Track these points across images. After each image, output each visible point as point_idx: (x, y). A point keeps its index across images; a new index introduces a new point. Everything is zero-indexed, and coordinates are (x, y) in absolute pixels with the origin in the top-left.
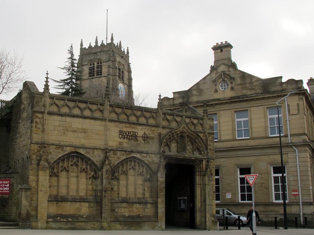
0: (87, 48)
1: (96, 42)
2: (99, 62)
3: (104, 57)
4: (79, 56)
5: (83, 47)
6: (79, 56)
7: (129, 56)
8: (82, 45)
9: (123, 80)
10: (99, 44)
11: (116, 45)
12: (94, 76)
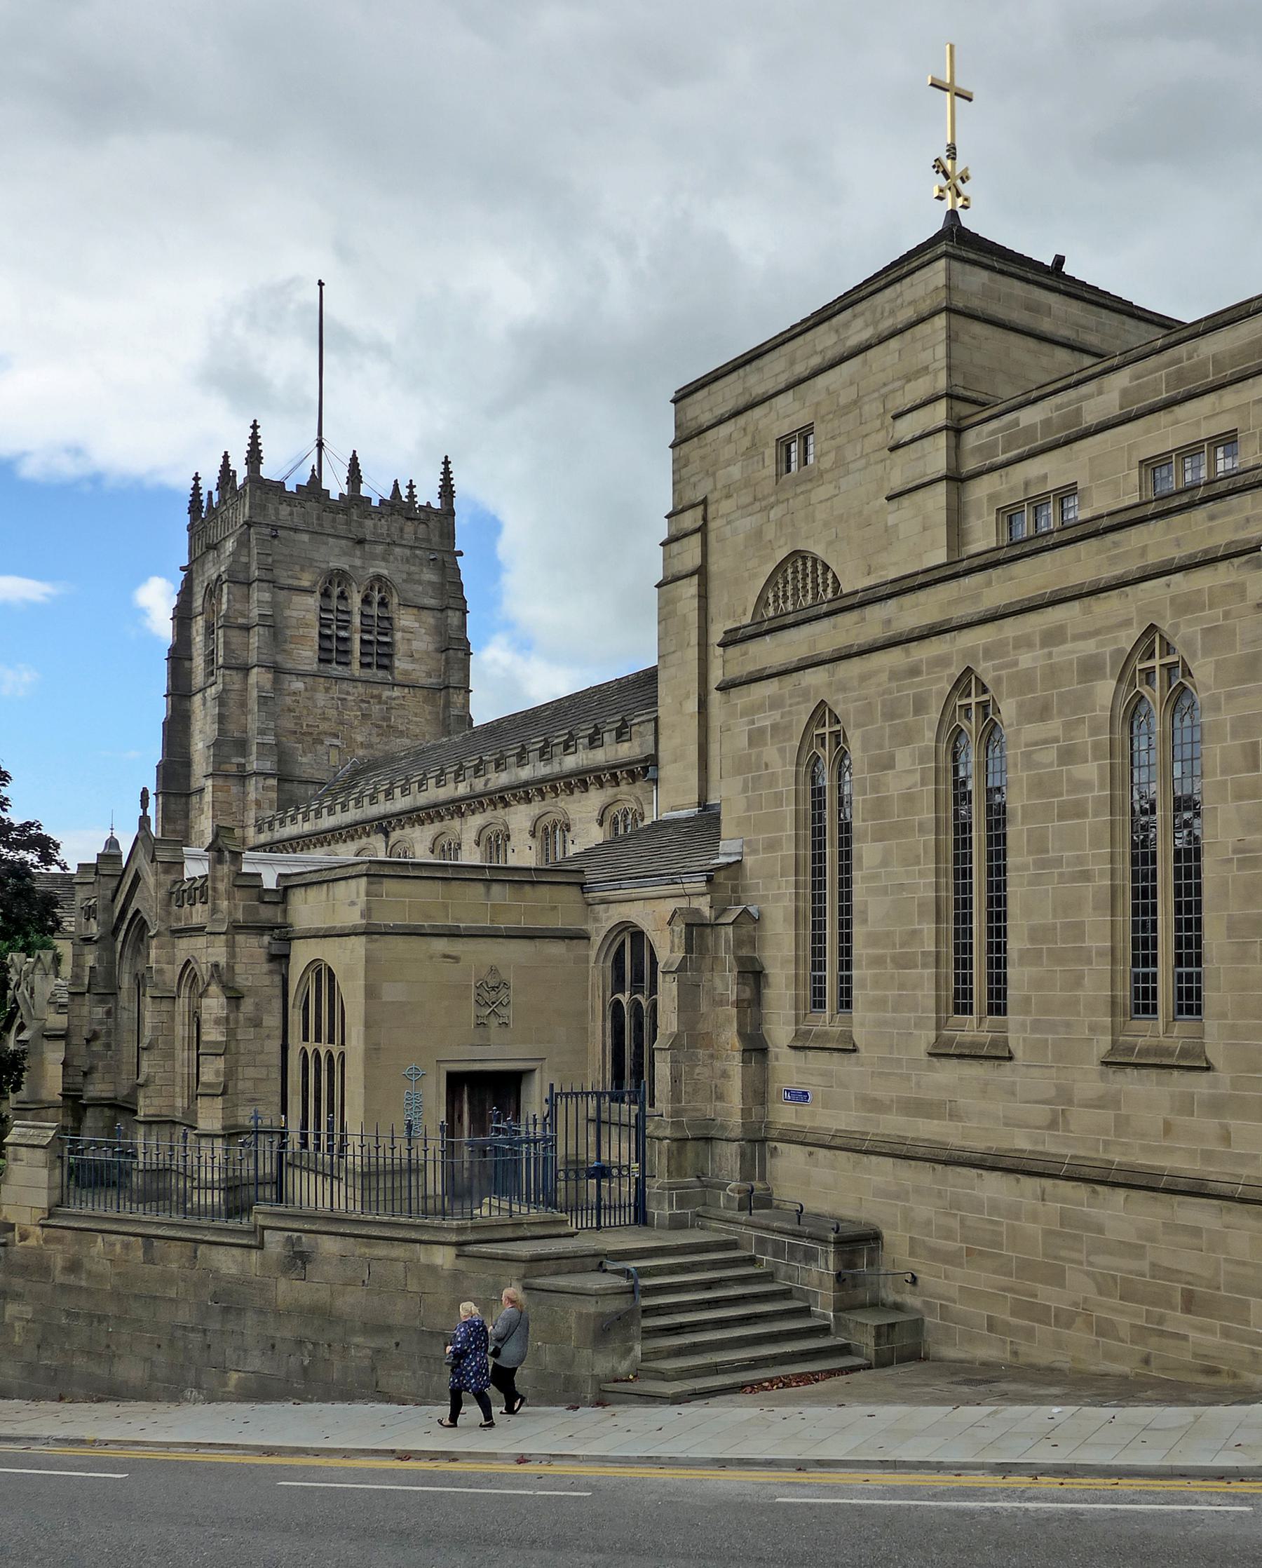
0: (290, 487)
2: (376, 597)
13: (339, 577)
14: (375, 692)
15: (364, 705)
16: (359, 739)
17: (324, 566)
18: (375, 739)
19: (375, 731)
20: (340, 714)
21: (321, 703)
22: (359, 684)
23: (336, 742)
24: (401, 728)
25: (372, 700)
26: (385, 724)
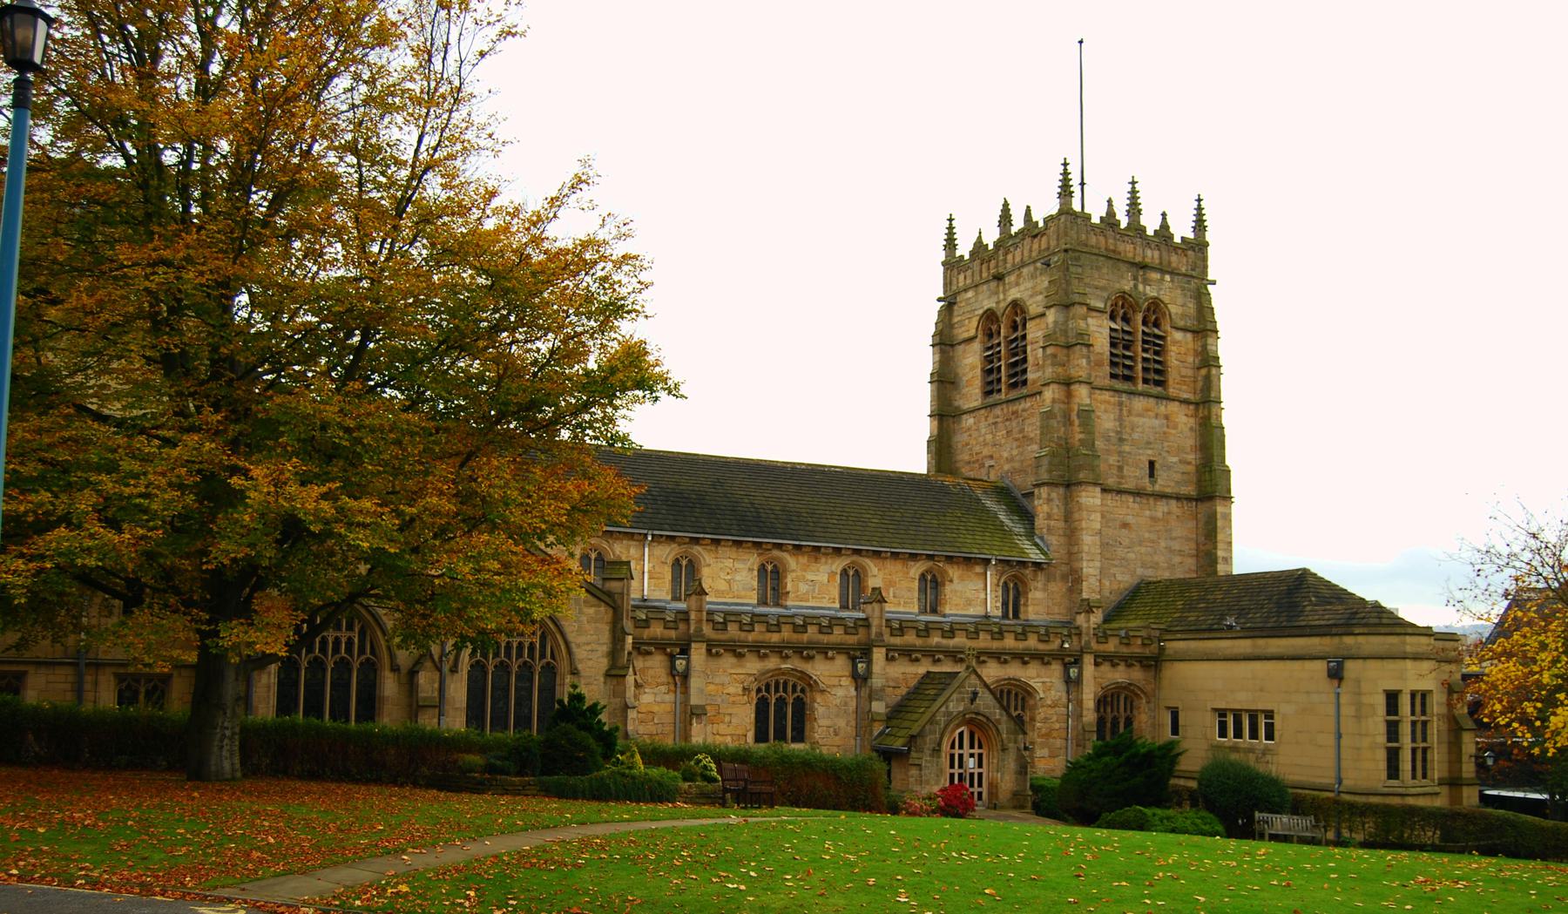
1: (1005, 218)
3: (1028, 289)
4: (939, 300)
5: (958, 254)
6: (939, 300)
7: (1207, 244)
8: (950, 243)
9: (1158, 383)
10: (1018, 224)
11: (1096, 213)
12: (999, 391)
13: (990, 316)
14: (1015, 408)
15: (1008, 423)
16: (1005, 455)
17: (981, 312)
18: (1015, 452)
19: (1015, 444)
20: (994, 436)
21: (983, 431)
22: (1004, 406)
23: (992, 463)
24: (1032, 435)
25: (1013, 417)
26: (1021, 436)
